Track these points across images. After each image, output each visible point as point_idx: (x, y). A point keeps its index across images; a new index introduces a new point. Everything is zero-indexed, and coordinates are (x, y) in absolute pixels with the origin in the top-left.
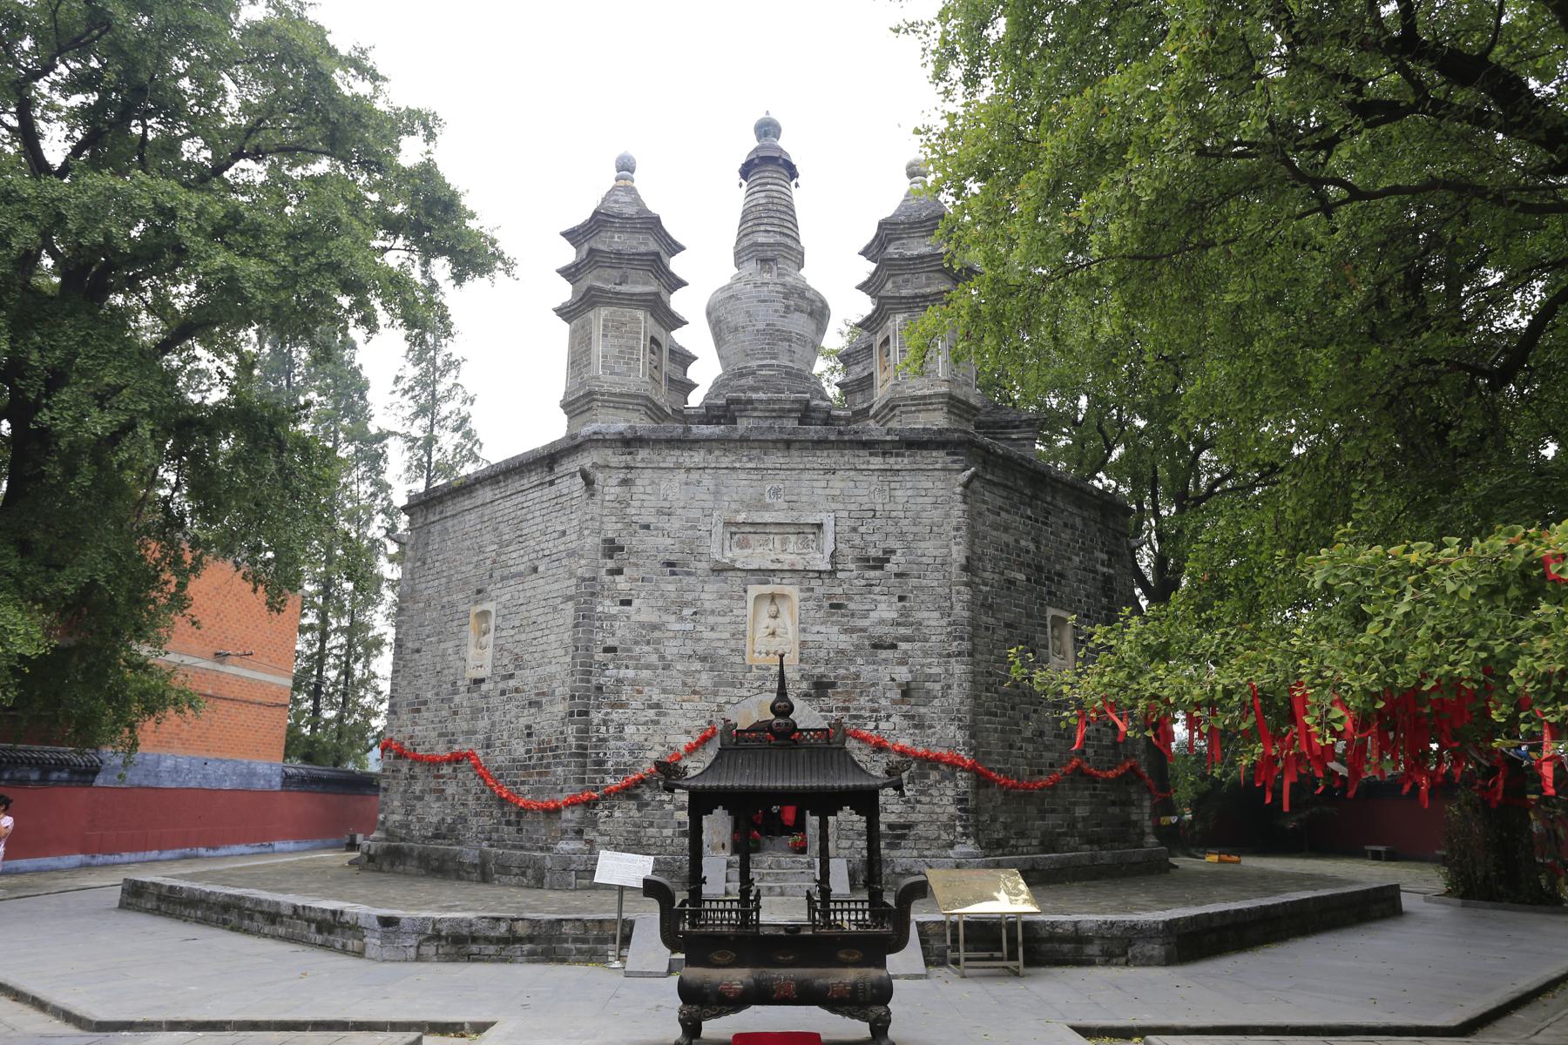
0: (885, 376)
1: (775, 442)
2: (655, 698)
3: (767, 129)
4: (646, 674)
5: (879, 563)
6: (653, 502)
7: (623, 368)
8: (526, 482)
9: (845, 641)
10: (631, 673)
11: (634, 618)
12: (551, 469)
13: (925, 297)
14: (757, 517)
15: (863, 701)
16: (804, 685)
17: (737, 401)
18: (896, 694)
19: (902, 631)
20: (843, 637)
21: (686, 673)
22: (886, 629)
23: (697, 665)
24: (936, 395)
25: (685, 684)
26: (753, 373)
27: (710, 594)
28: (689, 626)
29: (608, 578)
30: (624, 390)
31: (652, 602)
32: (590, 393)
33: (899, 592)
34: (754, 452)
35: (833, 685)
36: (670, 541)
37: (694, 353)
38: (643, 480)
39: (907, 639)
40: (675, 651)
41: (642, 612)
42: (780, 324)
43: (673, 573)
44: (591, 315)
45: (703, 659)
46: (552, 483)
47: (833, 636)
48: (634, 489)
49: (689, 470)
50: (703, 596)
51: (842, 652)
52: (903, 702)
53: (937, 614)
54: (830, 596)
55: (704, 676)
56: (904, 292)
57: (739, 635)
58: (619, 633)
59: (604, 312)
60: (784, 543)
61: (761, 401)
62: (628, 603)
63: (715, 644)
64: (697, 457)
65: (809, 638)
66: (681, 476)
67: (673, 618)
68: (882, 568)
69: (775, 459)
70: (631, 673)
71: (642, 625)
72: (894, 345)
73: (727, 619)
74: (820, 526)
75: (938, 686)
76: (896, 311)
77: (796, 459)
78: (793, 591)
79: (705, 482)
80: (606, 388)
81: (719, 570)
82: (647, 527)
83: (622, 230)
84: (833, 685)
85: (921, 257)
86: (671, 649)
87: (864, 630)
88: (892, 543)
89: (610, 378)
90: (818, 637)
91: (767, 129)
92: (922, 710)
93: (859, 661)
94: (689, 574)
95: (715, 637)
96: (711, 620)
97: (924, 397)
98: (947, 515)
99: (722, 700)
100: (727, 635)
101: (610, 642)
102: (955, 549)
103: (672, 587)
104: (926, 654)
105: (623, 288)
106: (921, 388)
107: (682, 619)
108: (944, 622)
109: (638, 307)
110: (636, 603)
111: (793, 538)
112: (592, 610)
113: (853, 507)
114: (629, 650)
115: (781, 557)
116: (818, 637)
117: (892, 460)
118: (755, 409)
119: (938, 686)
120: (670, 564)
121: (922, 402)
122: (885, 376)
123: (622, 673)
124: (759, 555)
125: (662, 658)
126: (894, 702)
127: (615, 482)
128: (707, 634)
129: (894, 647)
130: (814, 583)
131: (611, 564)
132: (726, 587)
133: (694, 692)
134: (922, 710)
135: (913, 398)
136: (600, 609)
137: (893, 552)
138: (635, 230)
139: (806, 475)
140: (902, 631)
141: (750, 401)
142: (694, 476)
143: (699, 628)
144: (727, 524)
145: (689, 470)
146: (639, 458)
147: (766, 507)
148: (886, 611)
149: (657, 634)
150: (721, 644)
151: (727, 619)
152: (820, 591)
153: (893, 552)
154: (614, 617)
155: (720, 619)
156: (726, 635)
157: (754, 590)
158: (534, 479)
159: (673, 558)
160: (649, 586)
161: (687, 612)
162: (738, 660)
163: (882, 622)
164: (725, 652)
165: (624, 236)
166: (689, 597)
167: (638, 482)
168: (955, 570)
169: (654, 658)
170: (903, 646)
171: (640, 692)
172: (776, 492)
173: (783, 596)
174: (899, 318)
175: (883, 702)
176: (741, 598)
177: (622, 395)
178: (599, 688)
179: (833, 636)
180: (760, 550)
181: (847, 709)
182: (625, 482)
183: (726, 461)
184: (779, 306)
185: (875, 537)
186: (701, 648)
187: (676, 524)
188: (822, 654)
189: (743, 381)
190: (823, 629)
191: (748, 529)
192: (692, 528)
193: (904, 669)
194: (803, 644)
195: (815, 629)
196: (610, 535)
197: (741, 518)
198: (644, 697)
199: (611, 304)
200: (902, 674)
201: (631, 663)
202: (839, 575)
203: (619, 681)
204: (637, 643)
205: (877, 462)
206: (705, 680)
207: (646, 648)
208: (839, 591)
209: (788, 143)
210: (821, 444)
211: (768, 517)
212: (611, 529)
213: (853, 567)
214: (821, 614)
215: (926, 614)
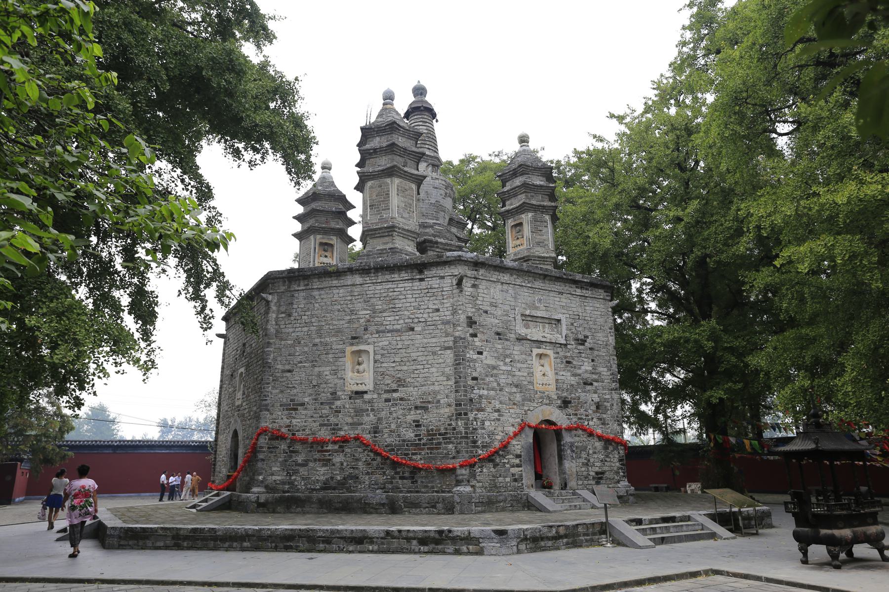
0: (518, 242)
1: (540, 275)
2: (497, 406)
3: (420, 91)
4: (492, 393)
5: (582, 342)
6: (488, 299)
7: (406, 215)
8: (396, 276)
9: (573, 380)
10: (485, 392)
11: (485, 362)
12: (421, 272)
13: (544, 206)
14: (534, 313)
15: (582, 410)
16: (559, 402)
17: (430, 241)
18: (594, 408)
19: (594, 376)
20: (572, 378)
21: (511, 393)
22: (588, 375)
23: (514, 390)
24: (550, 257)
25: (510, 399)
26: (432, 227)
27: (517, 350)
28: (509, 368)
29: (470, 339)
30: (410, 228)
31: (492, 354)
32: (393, 227)
33: (591, 357)
34: (530, 278)
35: (570, 402)
36: (497, 321)
37: (353, 203)
38: (483, 285)
39: (597, 381)
40: (504, 381)
41: (488, 359)
42: (442, 202)
43: (500, 339)
44: (388, 180)
45: (517, 386)
46: (421, 280)
47: (568, 377)
48: (479, 291)
49: (502, 283)
50: (515, 352)
51: (572, 385)
52: (597, 412)
53: (605, 369)
54: (566, 357)
55: (518, 395)
56: (534, 202)
57: (531, 374)
58: (478, 370)
59: (397, 181)
60: (544, 328)
61: (442, 243)
62: (480, 353)
63: (522, 378)
64: (506, 277)
65: (560, 377)
66: (499, 286)
67: (502, 363)
68: (583, 344)
69: (538, 284)
70: (485, 392)
71: (489, 366)
72: (527, 229)
73: (525, 366)
74: (559, 321)
75: (608, 404)
76: (528, 211)
77: (547, 285)
78: (550, 353)
79: (510, 291)
80: (401, 225)
81: (521, 339)
82: (486, 312)
83: (403, 136)
84: (570, 402)
85: (541, 186)
86: (503, 380)
87: (580, 375)
88: (588, 334)
89: (401, 220)
90: (563, 378)
91: (420, 91)
92: (604, 416)
93: (579, 391)
94: (507, 340)
95: (521, 375)
96: (519, 365)
97: (544, 257)
98: (606, 322)
99: (526, 408)
100: (526, 374)
101: (475, 375)
102: (610, 338)
103: (500, 346)
104: (604, 389)
105: (406, 169)
106: (540, 252)
107: (505, 364)
108: (609, 373)
109: (413, 182)
110: (485, 353)
111: (547, 325)
112: (465, 356)
113: (571, 313)
114: (483, 380)
115: (546, 335)
116: (563, 378)
117: (584, 291)
118: (438, 247)
119: (608, 404)
120: (498, 334)
121: (543, 259)
122: (518, 242)
123: (482, 392)
124: (536, 332)
125: (499, 385)
126: (594, 412)
127: (470, 285)
128: (517, 373)
129: (591, 384)
130: (559, 350)
131: (471, 331)
132: (523, 349)
133: (514, 404)
134: (604, 416)
135: (539, 257)
136: (468, 356)
137: (587, 337)
138: (409, 138)
139: (552, 294)
140: (594, 376)
141: (437, 243)
142: (505, 287)
143: (514, 369)
144: (522, 315)
145: (502, 283)
146: (480, 273)
147: (537, 308)
148: (587, 367)
149: (495, 371)
150: (523, 378)
151: (525, 366)
152: (562, 354)
153: (587, 337)
154: (474, 361)
155: (522, 366)
156: (526, 374)
157: (536, 351)
158: (405, 275)
159: (499, 330)
160: (490, 345)
161: (508, 360)
162: (531, 387)
163: (586, 371)
164: (526, 383)
165: (404, 139)
166: (508, 352)
167: (480, 286)
168: (611, 348)
169: (495, 384)
170: (595, 384)
171: (490, 403)
172: (540, 300)
173: (546, 355)
174: (530, 215)
175: (590, 412)
176: (530, 355)
177: (408, 231)
178: (471, 400)
179: (568, 377)
180: (534, 330)
181: (576, 415)
182: (474, 286)
183: (519, 281)
184: (443, 192)
185: (580, 329)
186: (515, 380)
187: (499, 312)
188: (565, 386)
189: (427, 230)
190: (564, 373)
191: (529, 319)
192: (507, 315)
193: (596, 395)
194: (557, 380)
195: (561, 373)
196: (470, 315)
197: (528, 312)
198: (492, 406)
199: (401, 177)
200: (596, 397)
201: (485, 387)
202: (569, 346)
203: (480, 396)
204: (487, 376)
205: (579, 292)
206: (518, 397)
207: (491, 379)
208: (568, 354)
209: (430, 98)
210: (558, 279)
211: (539, 314)
212: (470, 311)
213: (573, 343)
214: (563, 366)
215: (602, 369)
